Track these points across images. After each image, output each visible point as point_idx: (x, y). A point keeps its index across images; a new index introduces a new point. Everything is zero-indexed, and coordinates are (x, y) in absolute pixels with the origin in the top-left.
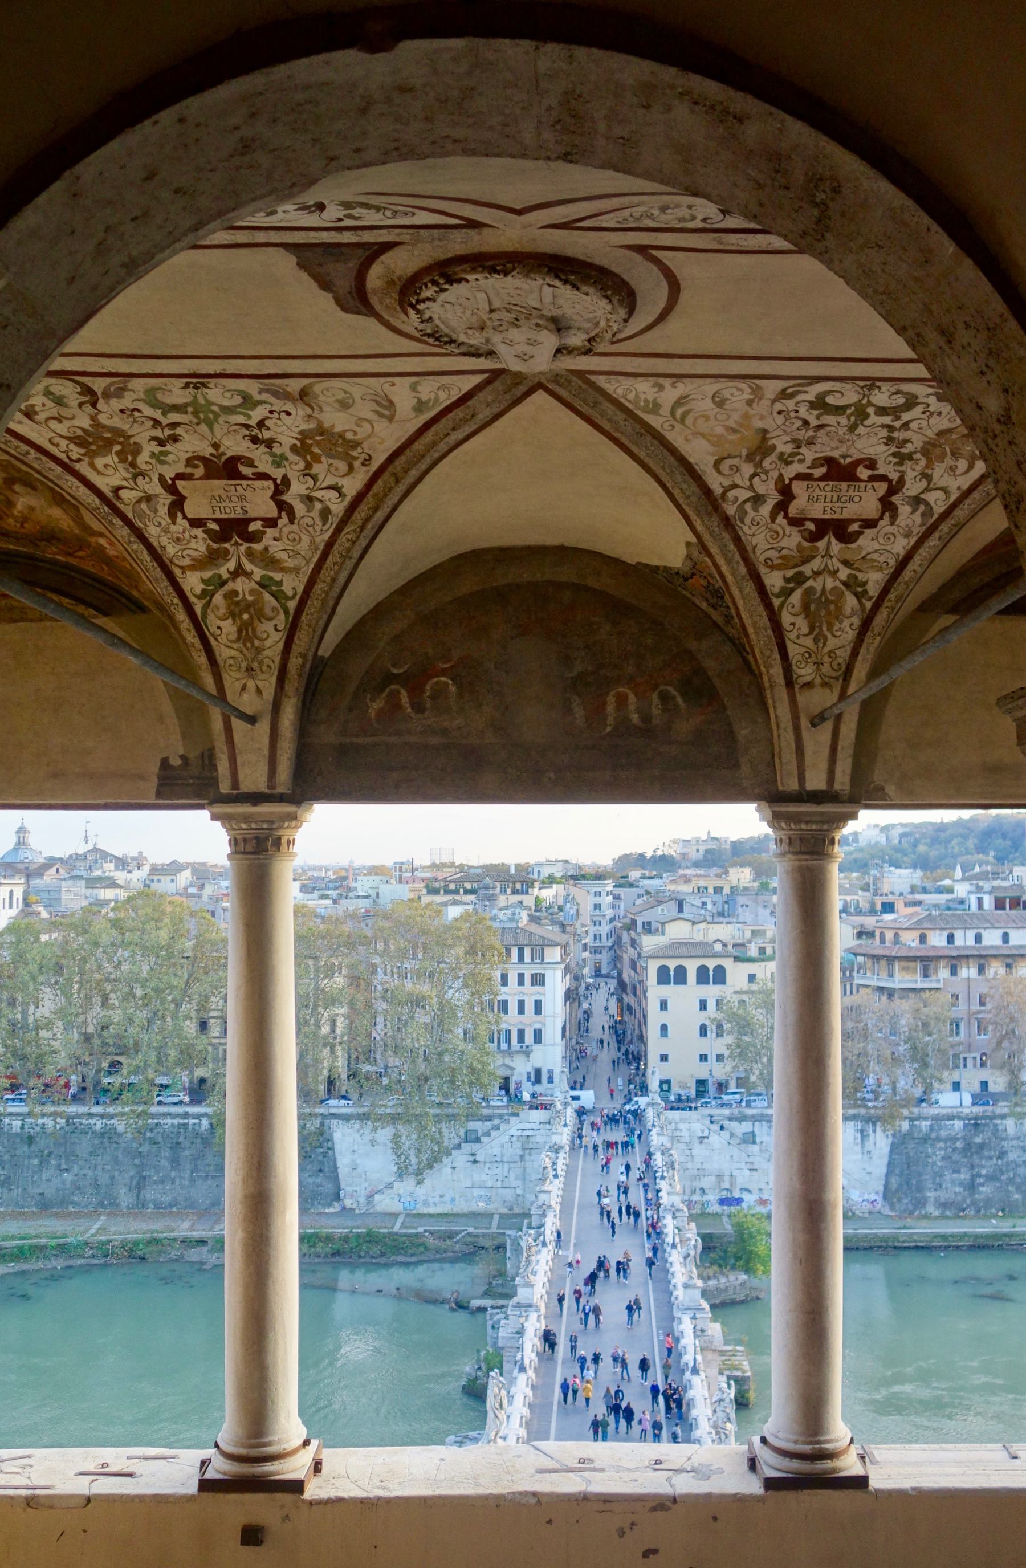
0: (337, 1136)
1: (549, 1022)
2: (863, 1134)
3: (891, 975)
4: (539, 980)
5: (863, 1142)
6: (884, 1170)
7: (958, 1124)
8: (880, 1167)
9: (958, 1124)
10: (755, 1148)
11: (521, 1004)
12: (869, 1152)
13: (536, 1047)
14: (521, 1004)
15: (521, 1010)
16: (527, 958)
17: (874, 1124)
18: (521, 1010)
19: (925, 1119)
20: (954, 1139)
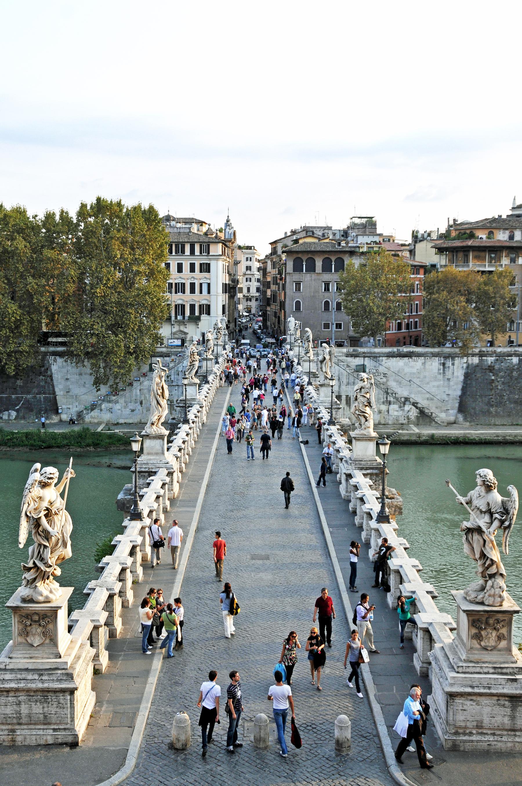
0: (54, 368)
4: (206, 268)
5: (444, 373)
6: (459, 393)
7: (515, 360)
12: (449, 379)
13: (204, 317)
16: (197, 252)
17: (453, 358)
20: (511, 369)
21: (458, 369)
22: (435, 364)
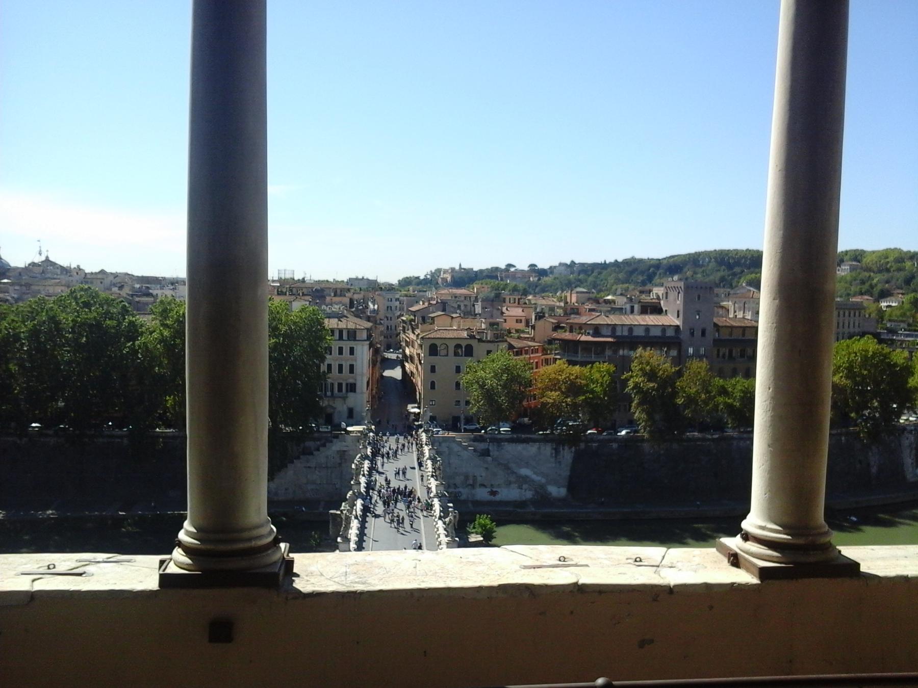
1: (359, 378)
2: (557, 451)
3: (577, 353)
7: (615, 445)
8: (566, 472)
9: (615, 445)
10: (489, 459)
11: (341, 366)
13: (351, 395)
14: (341, 366)
15: (340, 371)
17: (563, 445)
18: (340, 371)
19: (594, 442)
21: (567, 455)
22: (548, 449)
